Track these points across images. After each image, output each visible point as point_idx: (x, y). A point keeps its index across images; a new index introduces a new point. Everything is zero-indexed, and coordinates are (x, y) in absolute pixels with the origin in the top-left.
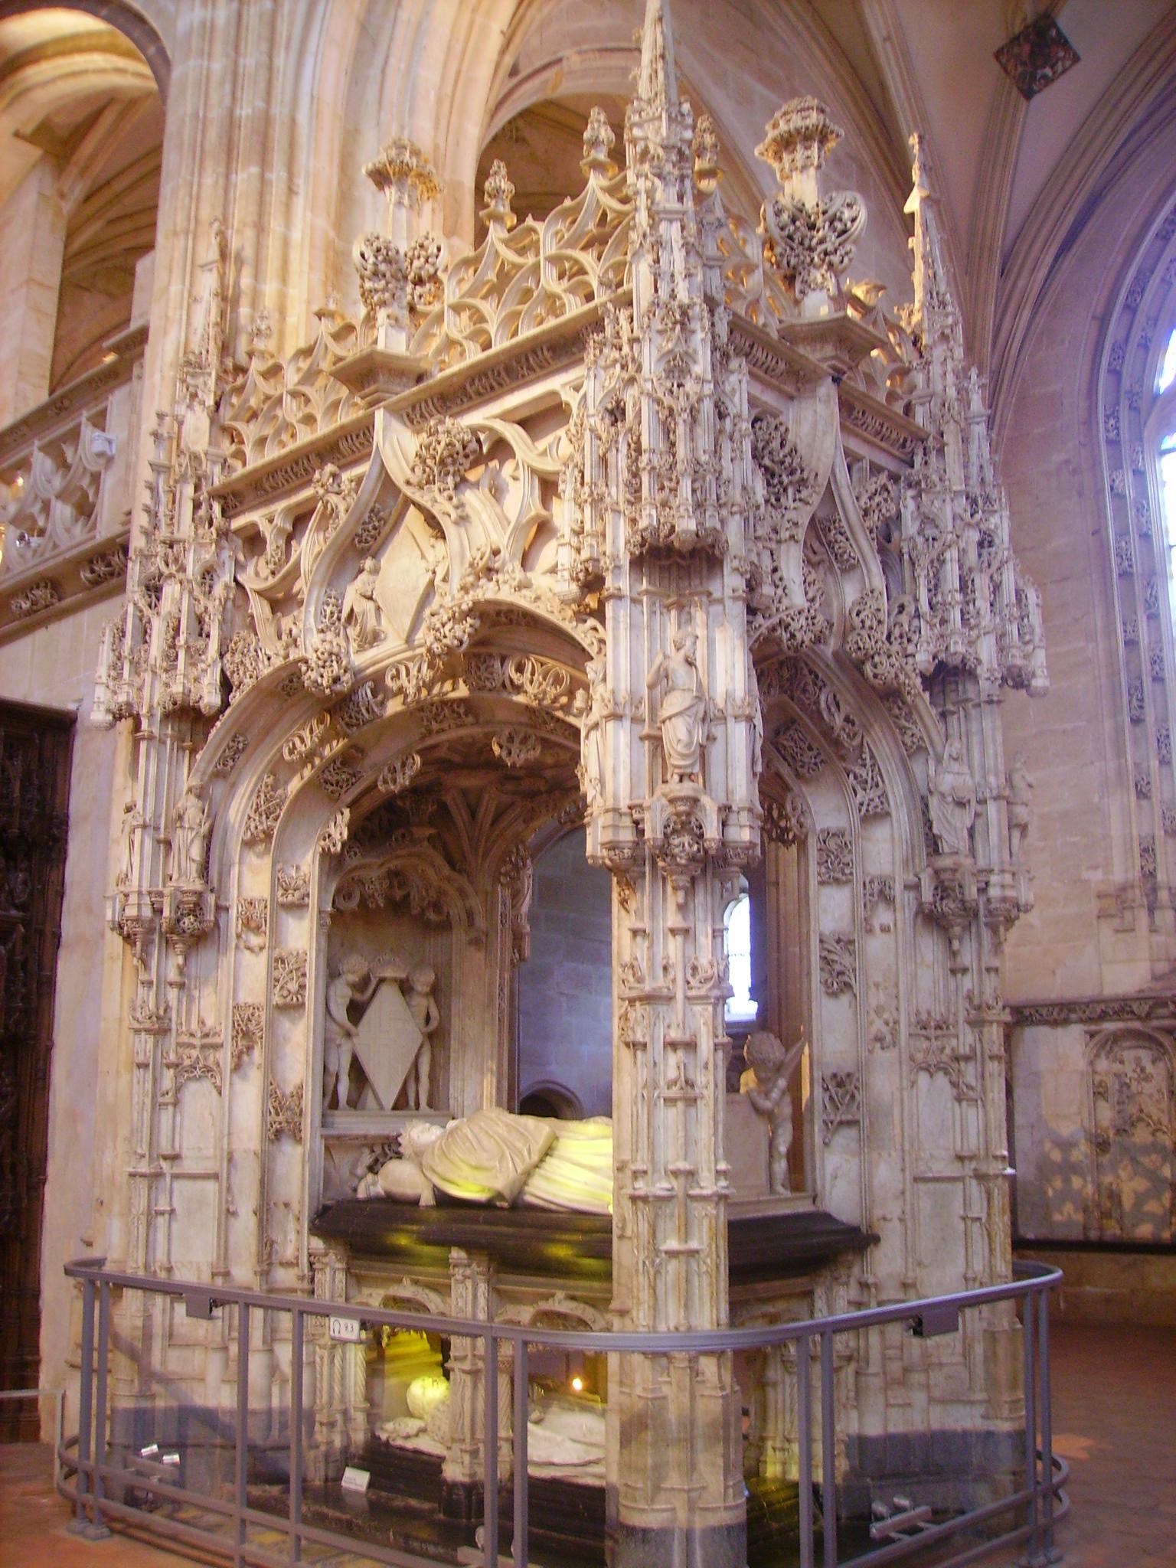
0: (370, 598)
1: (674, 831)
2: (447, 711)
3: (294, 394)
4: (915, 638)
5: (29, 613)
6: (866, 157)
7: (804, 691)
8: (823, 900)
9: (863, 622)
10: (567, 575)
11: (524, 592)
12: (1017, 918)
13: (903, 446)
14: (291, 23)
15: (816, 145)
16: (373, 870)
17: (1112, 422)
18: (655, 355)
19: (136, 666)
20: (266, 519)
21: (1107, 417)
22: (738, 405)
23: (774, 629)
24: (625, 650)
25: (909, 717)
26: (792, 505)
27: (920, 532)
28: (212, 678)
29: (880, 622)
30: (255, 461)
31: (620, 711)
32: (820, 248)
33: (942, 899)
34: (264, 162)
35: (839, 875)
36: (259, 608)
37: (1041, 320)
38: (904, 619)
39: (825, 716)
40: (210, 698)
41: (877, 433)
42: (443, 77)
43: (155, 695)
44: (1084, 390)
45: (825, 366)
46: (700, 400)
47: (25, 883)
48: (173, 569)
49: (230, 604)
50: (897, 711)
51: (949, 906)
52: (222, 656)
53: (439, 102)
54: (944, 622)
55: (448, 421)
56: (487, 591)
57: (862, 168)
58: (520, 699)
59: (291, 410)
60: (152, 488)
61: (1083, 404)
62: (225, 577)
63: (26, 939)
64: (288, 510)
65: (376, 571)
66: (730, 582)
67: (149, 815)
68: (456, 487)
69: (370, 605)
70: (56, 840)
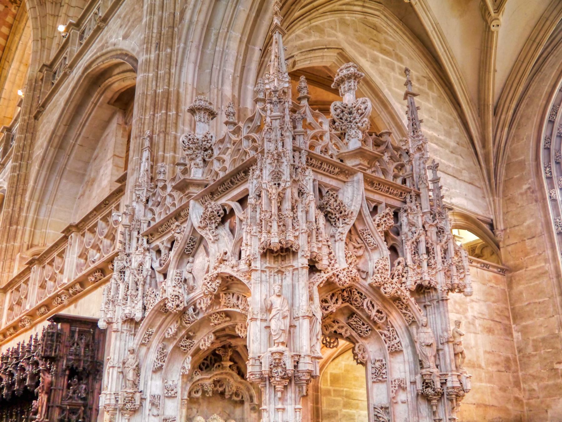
0: (191, 273)
1: (274, 366)
2: (219, 316)
3: (170, 195)
4: (405, 275)
5: (94, 282)
6: (431, 76)
7: (356, 301)
8: (375, 390)
9: (378, 270)
11: (235, 269)
12: (464, 396)
13: (401, 195)
14: (177, 57)
15: (353, 81)
16: (207, 379)
17: (548, 169)
18: (268, 173)
19: (113, 302)
20: (161, 242)
21: (546, 168)
22: (309, 188)
23: (331, 277)
24: (261, 290)
25: (406, 308)
26: (341, 225)
27: (409, 230)
28: (140, 305)
29: (387, 270)
30: (158, 220)
31: (255, 317)
32: (354, 121)
33: (426, 388)
34: (167, 109)
35: (380, 378)
36: (159, 278)
37: (513, 131)
38: (400, 267)
39: (367, 310)
40: (138, 316)
41: (387, 192)
42: (235, 70)
43: (120, 313)
44: (534, 157)
45: (356, 168)
46: (284, 189)
47: (85, 389)
48: (129, 264)
49: (149, 277)
50: (400, 307)
51: (430, 391)
52: (143, 297)
53: (234, 79)
54: (419, 266)
55: (213, 203)
57: (430, 80)
58: (238, 310)
59: (169, 200)
60: (123, 234)
61: (534, 163)
62: (147, 266)
63: (84, 412)
64: (168, 240)
65: (193, 262)
66: (301, 261)
67: (116, 362)
68: (216, 228)
69: (190, 276)
70: (98, 371)
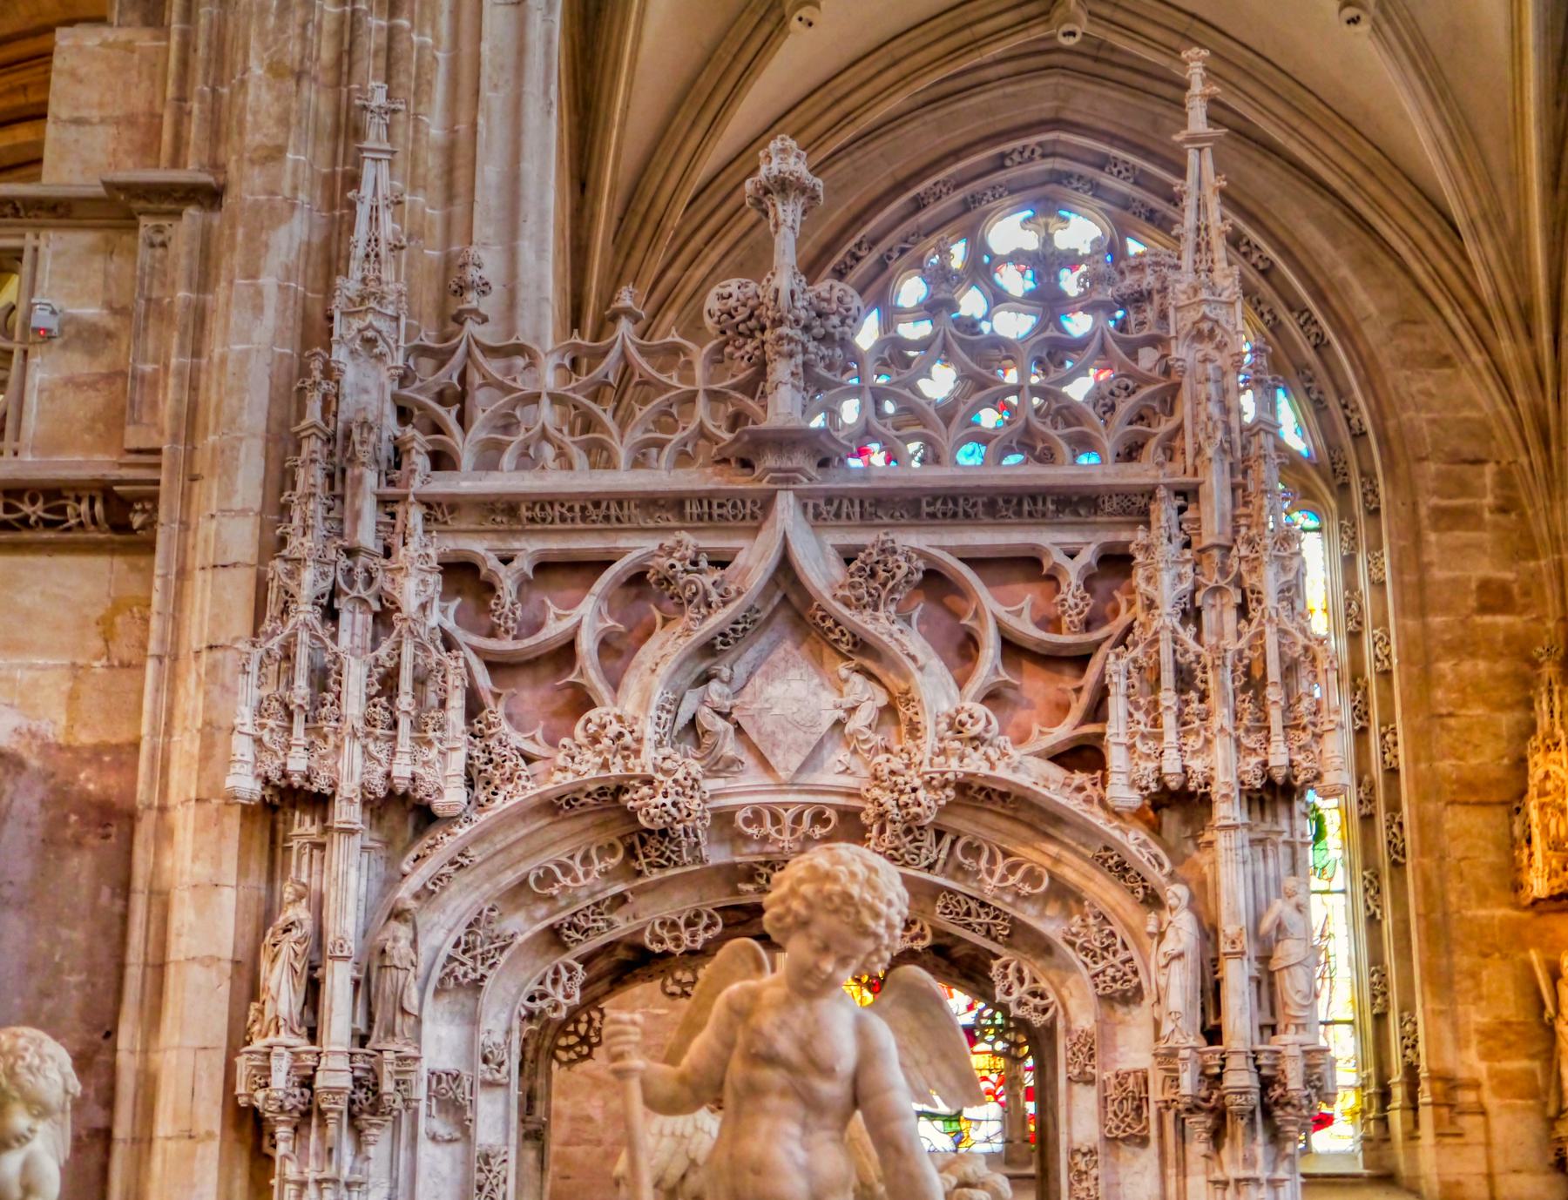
0: (726, 716)
10: (1123, 779)
56: (976, 764)
